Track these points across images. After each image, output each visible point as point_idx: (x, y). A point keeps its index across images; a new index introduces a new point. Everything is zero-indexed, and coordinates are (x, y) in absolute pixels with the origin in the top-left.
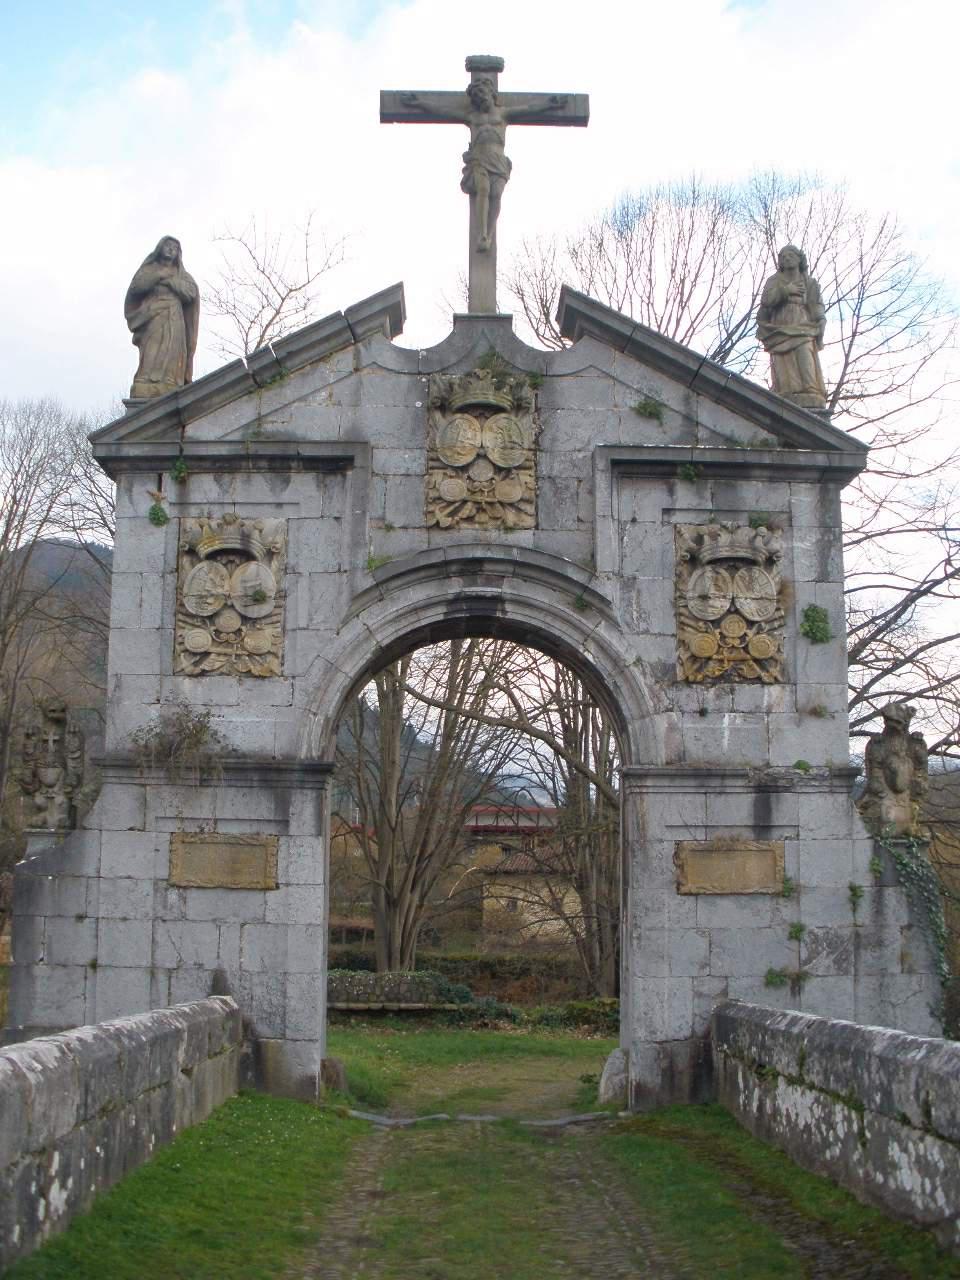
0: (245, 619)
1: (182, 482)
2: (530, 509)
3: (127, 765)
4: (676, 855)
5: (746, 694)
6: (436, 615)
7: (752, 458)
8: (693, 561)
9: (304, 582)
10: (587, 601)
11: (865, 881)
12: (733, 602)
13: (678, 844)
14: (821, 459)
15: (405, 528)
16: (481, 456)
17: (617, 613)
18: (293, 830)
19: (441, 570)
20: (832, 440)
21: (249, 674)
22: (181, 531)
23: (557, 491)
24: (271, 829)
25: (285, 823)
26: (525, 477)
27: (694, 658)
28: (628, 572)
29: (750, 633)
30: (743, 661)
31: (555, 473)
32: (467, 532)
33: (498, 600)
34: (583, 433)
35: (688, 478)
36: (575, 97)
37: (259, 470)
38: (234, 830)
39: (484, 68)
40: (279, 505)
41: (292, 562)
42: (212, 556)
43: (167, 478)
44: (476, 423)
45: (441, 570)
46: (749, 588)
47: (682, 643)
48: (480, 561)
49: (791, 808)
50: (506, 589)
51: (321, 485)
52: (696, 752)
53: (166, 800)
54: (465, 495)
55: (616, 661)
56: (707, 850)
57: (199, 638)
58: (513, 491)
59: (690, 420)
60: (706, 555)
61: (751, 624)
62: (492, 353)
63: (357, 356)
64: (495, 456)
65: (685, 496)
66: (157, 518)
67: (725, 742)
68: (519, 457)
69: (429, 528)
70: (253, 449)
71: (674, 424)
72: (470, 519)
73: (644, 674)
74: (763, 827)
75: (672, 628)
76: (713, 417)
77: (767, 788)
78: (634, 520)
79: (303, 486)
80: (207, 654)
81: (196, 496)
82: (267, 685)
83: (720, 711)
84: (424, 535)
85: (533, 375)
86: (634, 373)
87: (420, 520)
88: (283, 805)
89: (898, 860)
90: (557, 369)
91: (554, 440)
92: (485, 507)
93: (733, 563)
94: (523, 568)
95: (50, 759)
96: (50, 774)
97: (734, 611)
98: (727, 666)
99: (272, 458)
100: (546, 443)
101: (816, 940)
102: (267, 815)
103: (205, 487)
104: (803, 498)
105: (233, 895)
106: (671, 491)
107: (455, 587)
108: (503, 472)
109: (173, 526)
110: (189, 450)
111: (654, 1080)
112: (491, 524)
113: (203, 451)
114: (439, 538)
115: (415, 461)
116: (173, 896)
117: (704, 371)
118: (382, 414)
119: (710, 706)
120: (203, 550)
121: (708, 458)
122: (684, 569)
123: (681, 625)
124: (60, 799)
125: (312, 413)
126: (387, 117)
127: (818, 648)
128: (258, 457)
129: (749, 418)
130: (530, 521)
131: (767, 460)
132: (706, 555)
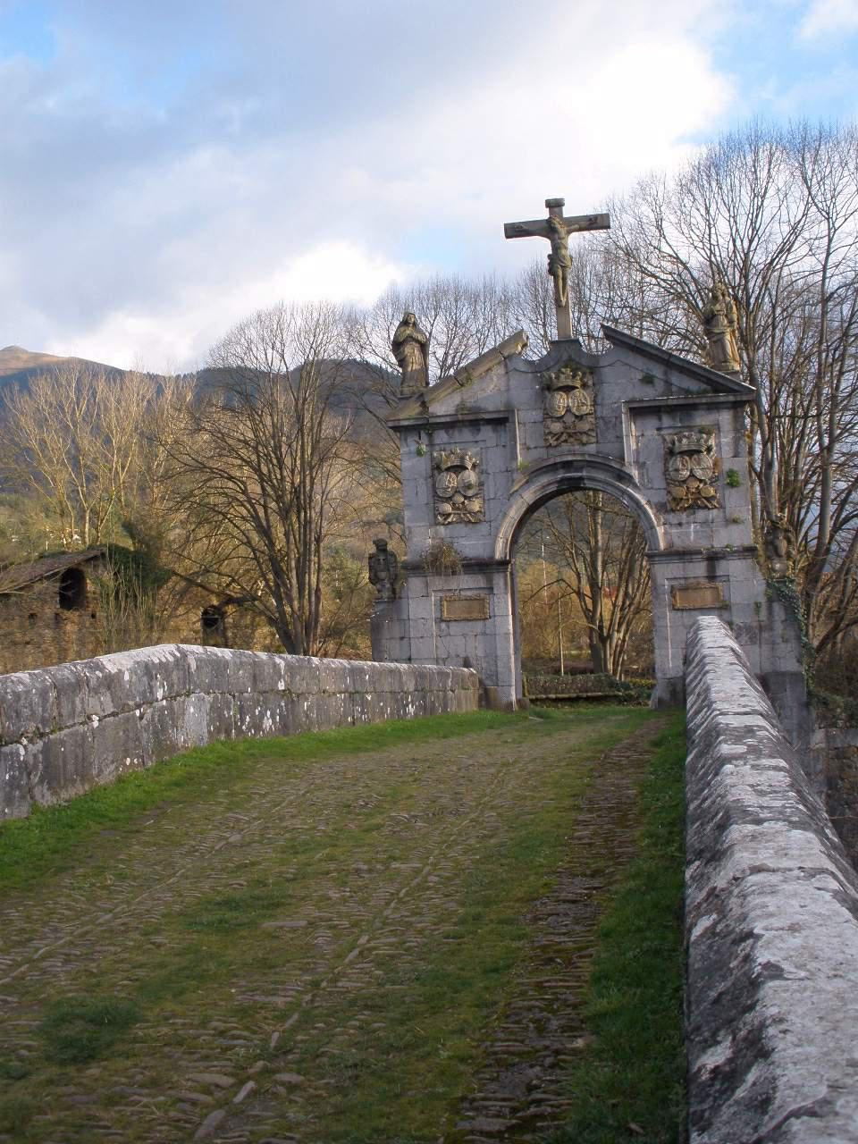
0: (466, 497)
1: (430, 435)
2: (594, 434)
3: (416, 568)
4: (671, 592)
5: (701, 515)
6: (553, 488)
7: (697, 401)
8: (671, 453)
9: (491, 477)
10: (623, 477)
11: (763, 600)
12: (691, 471)
13: (672, 587)
14: (731, 398)
15: (535, 448)
16: (568, 410)
17: (637, 481)
18: (495, 592)
19: (554, 467)
20: (736, 388)
21: (470, 522)
22: (432, 459)
23: (606, 423)
24: (486, 592)
25: (491, 589)
26: (590, 419)
27: (674, 499)
28: (641, 460)
29: (701, 485)
30: (699, 499)
31: (604, 415)
32: (565, 447)
33: (581, 479)
34: (617, 395)
35: (668, 413)
36: (602, 215)
37: (465, 426)
38: (469, 593)
39: (555, 205)
40: (476, 442)
41: (484, 467)
42: (448, 469)
43: (423, 435)
44: (565, 396)
45: (554, 467)
46: (699, 464)
47: (669, 492)
48: (571, 462)
49: (723, 567)
50: (584, 474)
51: (495, 431)
52: (679, 544)
53: (437, 582)
54: (562, 430)
55: (637, 502)
56: (685, 589)
57: (448, 508)
58: (585, 426)
59: (668, 383)
60: (677, 450)
61: (701, 481)
62: (570, 359)
63: (506, 366)
64: (574, 410)
65: (666, 421)
66: (419, 453)
67: (692, 538)
68: (585, 410)
69: (547, 447)
70: (460, 417)
71: (660, 385)
72: (566, 441)
73: (651, 508)
74: (712, 577)
75: (664, 486)
76: (679, 380)
77: (713, 558)
78: (643, 435)
79: (487, 433)
80: (450, 514)
81: (437, 441)
82: (478, 527)
83: (688, 523)
84: (544, 450)
85: (590, 368)
86: (640, 363)
87: (543, 444)
88: (490, 581)
89: (779, 589)
90: (601, 364)
91: (603, 399)
92: (572, 435)
93: (691, 453)
94: (591, 465)
95: (382, 567)
96: (383, 575)
97: (692, 475)
98: (690, 502)
99: (471, 421)
100: (599, 401)
101: (740, 628)
102: (482, 586)
103: (441, 437)
104: (725, 417)
105: (470, 623)
106: (660, 419)
107: (561, 475)
108: (580, 418)
109: (428, 456)
110: (432, 421)
111: (666, 696)
112: (575, 443)
113: (438, 420)
114: (551, 451)
115: (536, 415)
116: (443, 625)
117: (672, 360)
118: (522, 392)
119: (684, 521)
120: (444, 467)
121: (675, 402)
122: (668, 457)
123: (668, 484)
124: (388, 586)
125: (488, 392)
126: (508, 236)
127: (733, 491)
128: (463, 421)
129: (699, 380)
130: (594, 440)
131: (704, 401)
132: (677, 450)
